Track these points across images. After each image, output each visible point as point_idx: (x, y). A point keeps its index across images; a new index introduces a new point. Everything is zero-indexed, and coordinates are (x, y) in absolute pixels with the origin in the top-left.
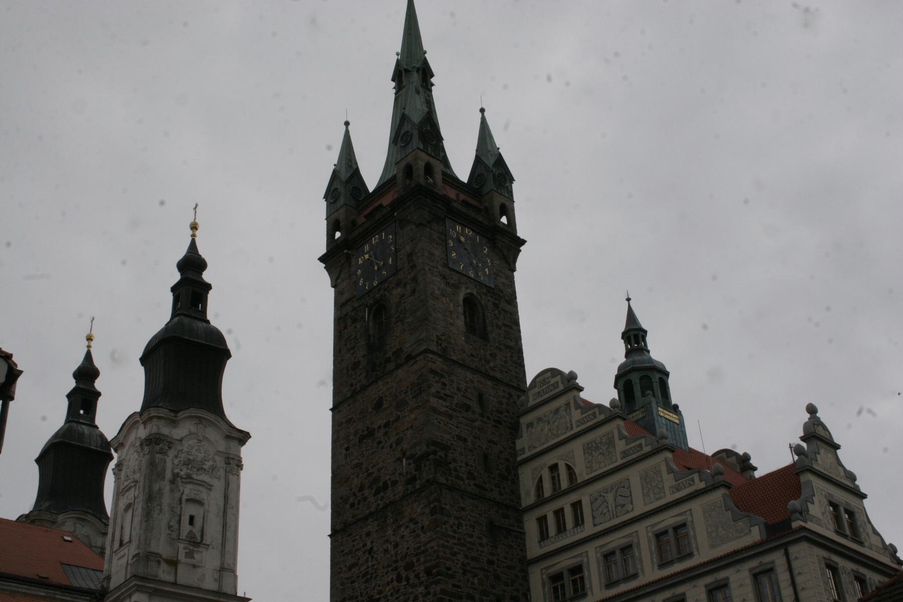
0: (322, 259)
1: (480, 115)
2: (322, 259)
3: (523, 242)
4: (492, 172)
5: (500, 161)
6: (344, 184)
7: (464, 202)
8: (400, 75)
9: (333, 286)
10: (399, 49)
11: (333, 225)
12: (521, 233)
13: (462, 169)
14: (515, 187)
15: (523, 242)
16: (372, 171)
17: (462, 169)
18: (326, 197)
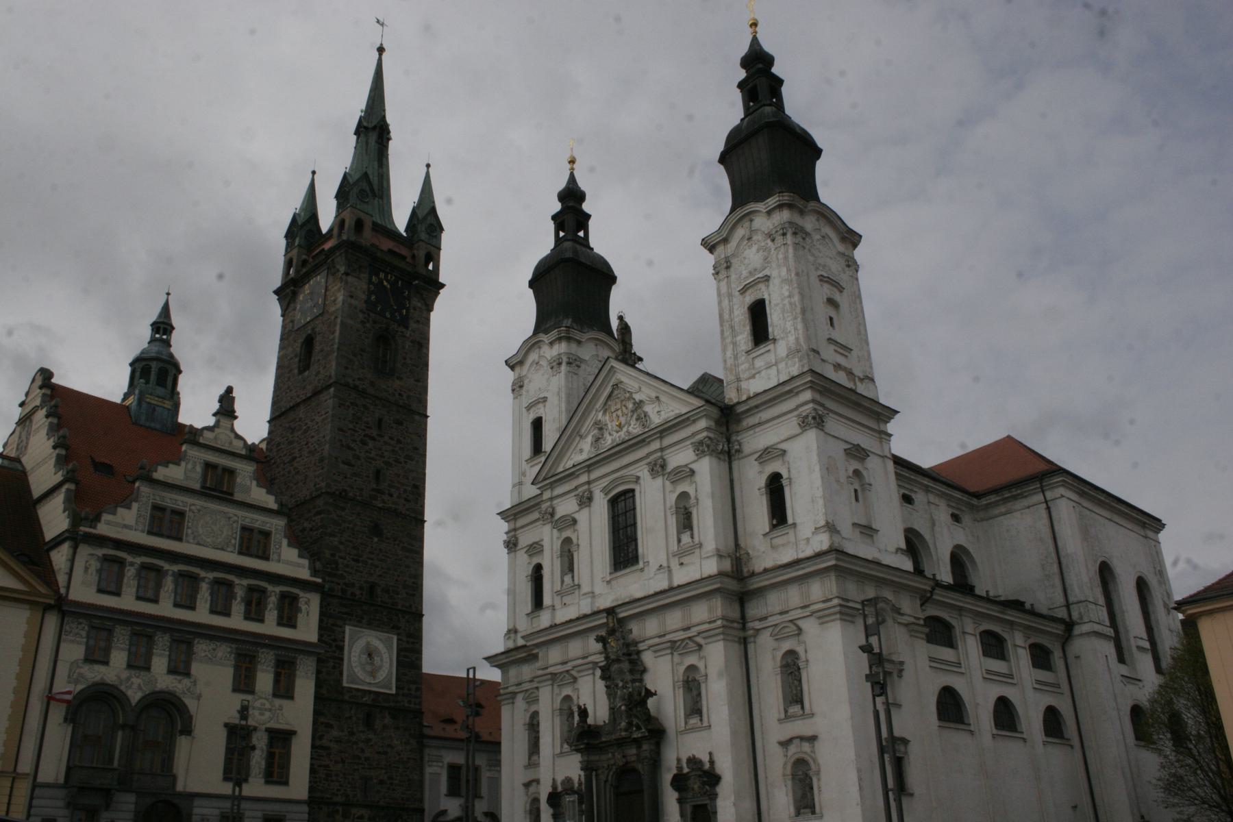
0: (276, 292)
1: (425, 169)
2: (276, 292)
3: (443, 286)
4: (427, 221)
5: (433, 210)
6: (303, 228)
7: (391, 252)
8: (362, 130)
9: (283, 315)
10: (363, 107)
11: (289, 264)
12: (441, 280)
13: (400, 220)
14: (444, 236)
15: (443, 286)
16: (327, 217)
17: (400, 220)
18: (286, 237)
